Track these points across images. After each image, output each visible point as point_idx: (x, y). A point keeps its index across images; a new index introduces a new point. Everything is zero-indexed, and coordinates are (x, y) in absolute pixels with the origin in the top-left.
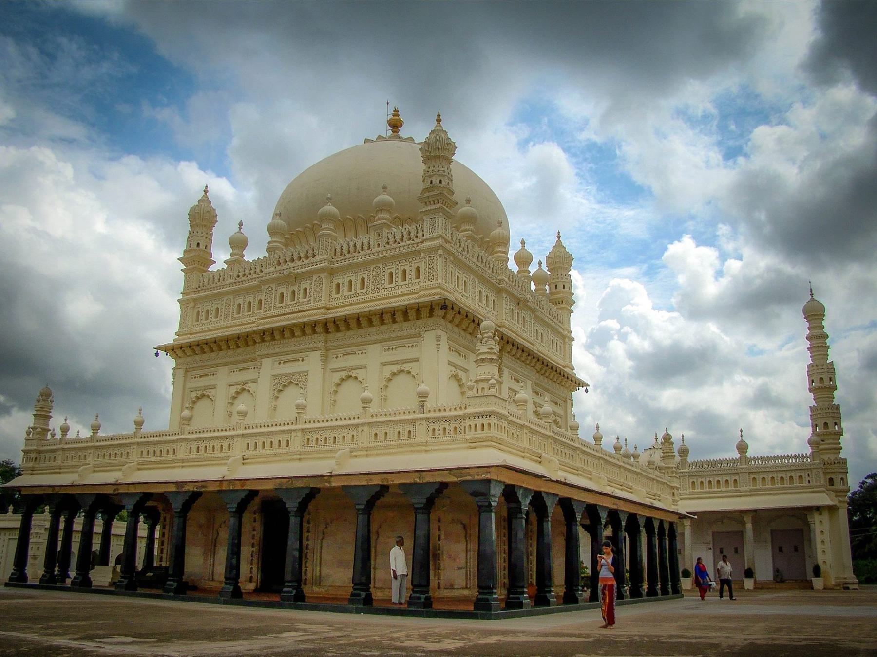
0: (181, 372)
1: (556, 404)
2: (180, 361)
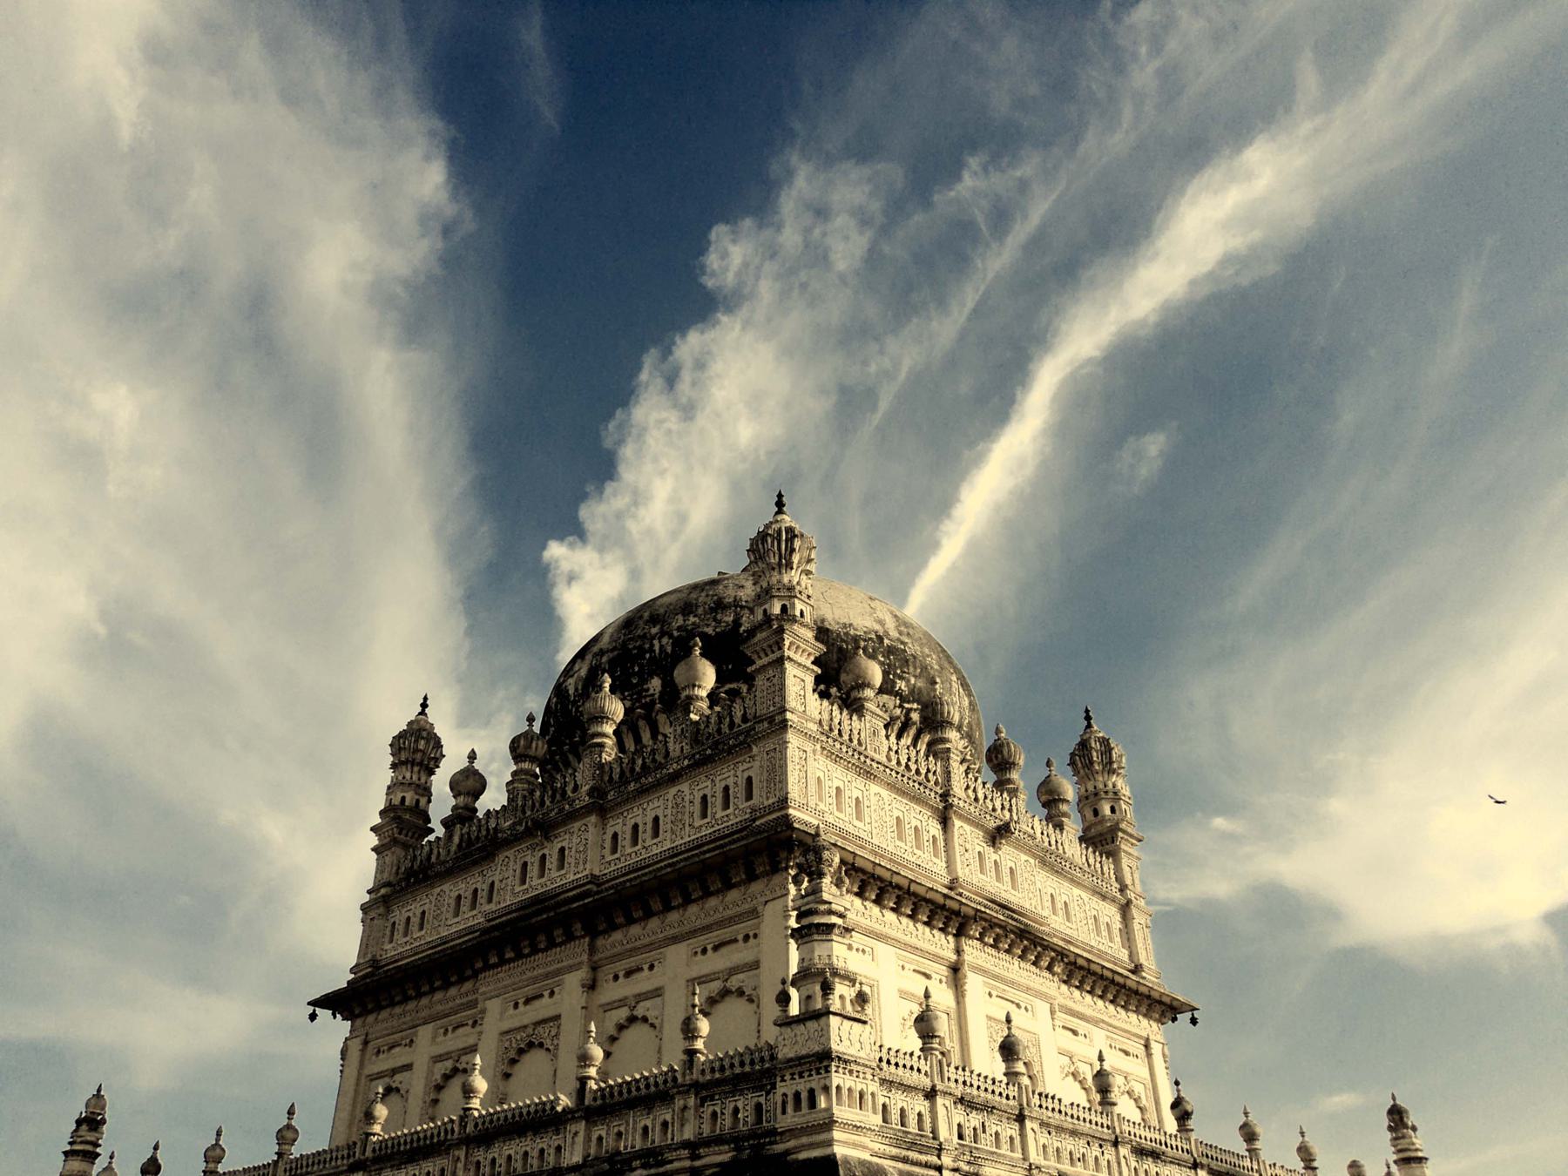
0: (356, 1045)
1: (1127, 1053)
2: (359, 1022)
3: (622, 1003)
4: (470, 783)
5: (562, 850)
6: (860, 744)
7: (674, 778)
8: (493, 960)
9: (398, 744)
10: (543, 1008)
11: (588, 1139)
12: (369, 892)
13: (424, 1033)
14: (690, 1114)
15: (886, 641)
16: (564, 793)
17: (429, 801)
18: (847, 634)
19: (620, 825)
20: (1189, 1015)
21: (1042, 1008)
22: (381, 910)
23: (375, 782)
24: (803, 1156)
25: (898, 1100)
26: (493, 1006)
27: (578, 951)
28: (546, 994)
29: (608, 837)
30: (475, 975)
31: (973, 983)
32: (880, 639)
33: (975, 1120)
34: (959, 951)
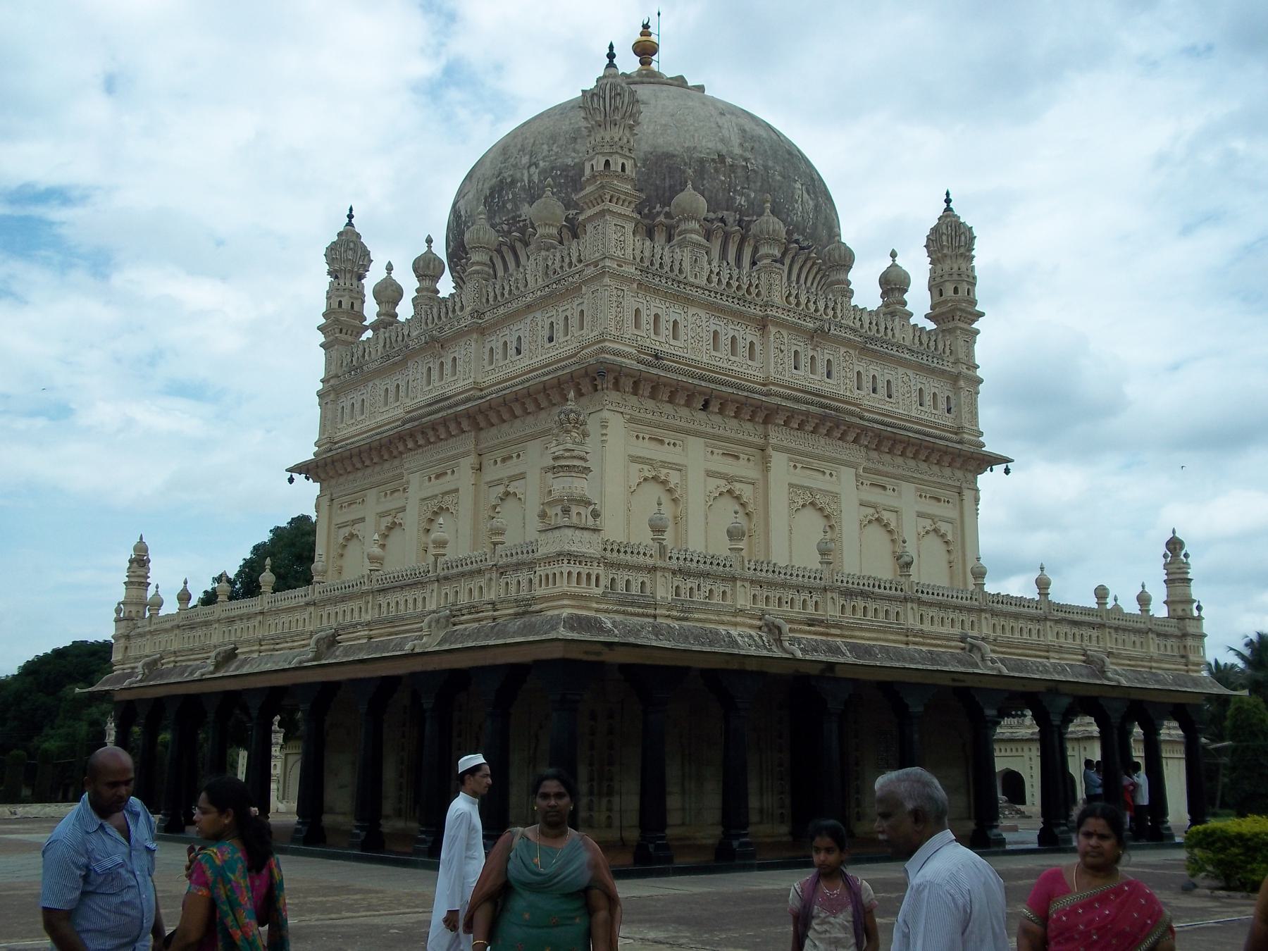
0: (326, 498)
1: (939, 500)
2: (325, 484)
3: (499, 482)
4: (389, 293)
5: (454, 359)
6: (681, 271)
7: (529, 307)
8: (410, 445)
9: (333, 253)
10: (447, 483)
11: (439, 593)
12: (322, 381)
13: (372, 495)
14: (493, 583)
15: (729, 160)
16: (454, 311)
17: (363, 302)
18: (691, 158)
19: (496, 342)
20: (1004, 466)
21: (848, 475)
22: (332, 396)
23: (315, 285)
24: (550, 613)
25: (622, 577)
26: (415, 481)
27: (466, 443)
28: (449, 472)
29: (487, 350)
30: (401, 453)
31: (779, 461)
32: (722, 158)
33: (692, 583)
34: (766, 437)
